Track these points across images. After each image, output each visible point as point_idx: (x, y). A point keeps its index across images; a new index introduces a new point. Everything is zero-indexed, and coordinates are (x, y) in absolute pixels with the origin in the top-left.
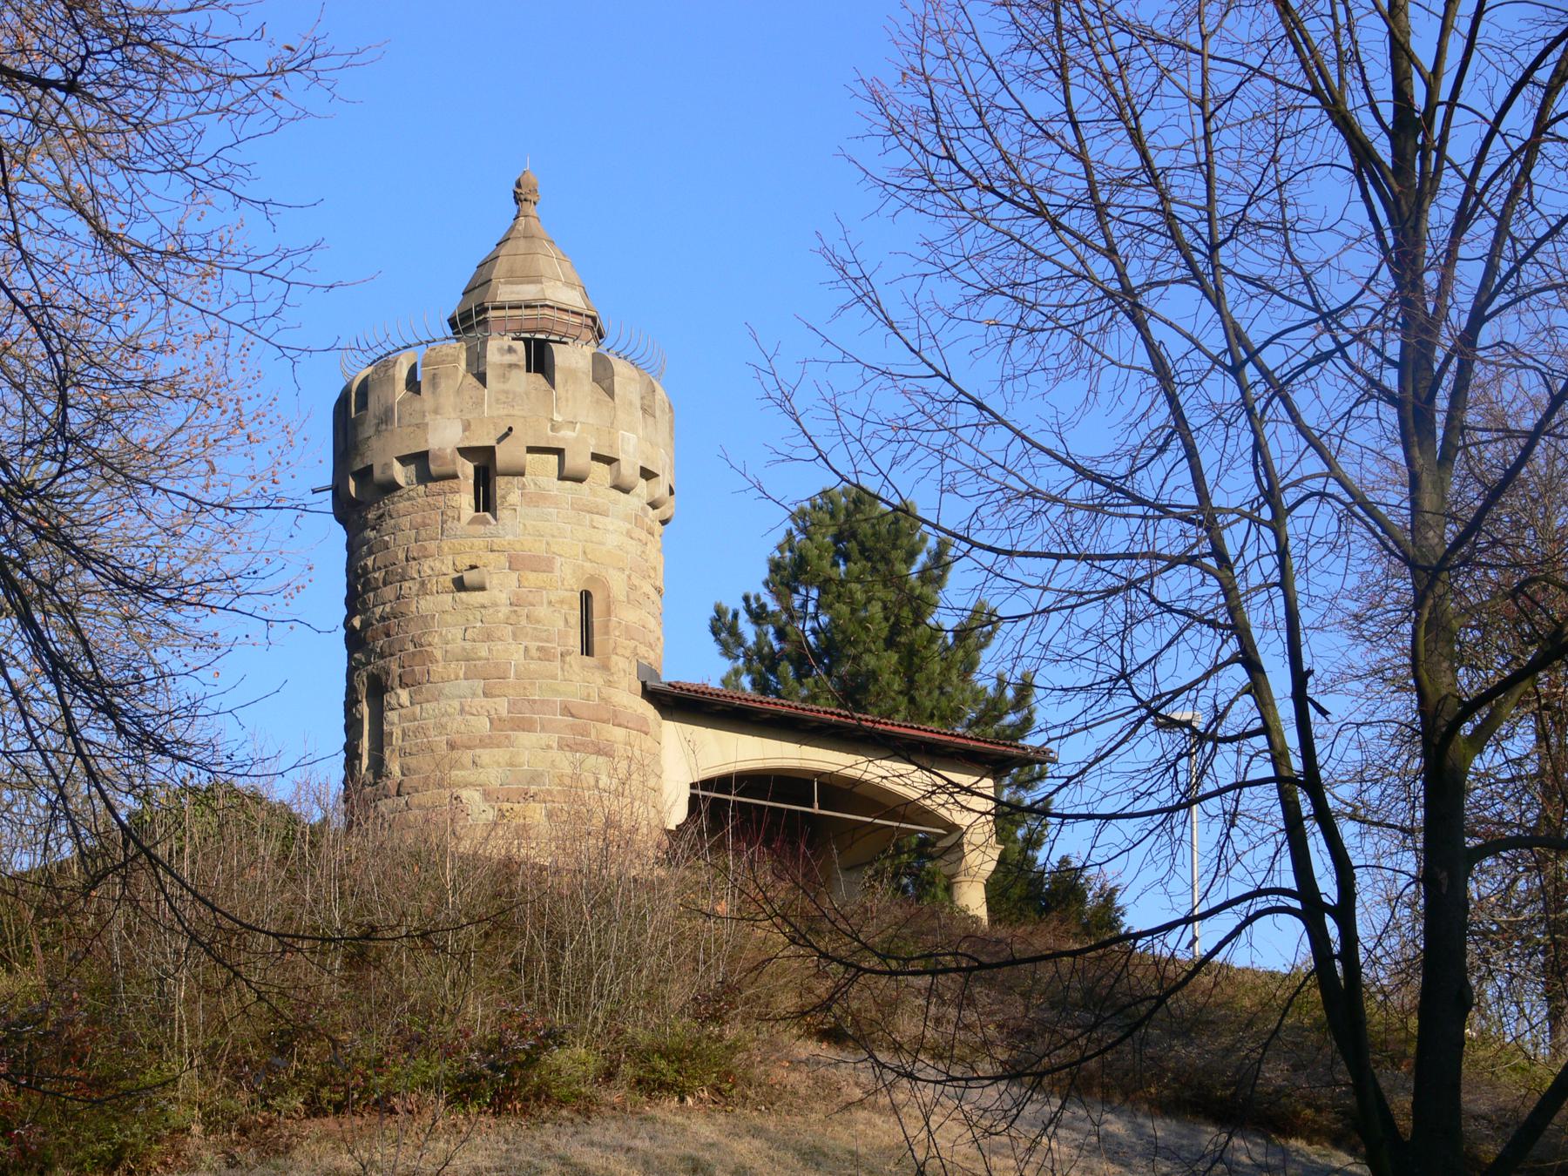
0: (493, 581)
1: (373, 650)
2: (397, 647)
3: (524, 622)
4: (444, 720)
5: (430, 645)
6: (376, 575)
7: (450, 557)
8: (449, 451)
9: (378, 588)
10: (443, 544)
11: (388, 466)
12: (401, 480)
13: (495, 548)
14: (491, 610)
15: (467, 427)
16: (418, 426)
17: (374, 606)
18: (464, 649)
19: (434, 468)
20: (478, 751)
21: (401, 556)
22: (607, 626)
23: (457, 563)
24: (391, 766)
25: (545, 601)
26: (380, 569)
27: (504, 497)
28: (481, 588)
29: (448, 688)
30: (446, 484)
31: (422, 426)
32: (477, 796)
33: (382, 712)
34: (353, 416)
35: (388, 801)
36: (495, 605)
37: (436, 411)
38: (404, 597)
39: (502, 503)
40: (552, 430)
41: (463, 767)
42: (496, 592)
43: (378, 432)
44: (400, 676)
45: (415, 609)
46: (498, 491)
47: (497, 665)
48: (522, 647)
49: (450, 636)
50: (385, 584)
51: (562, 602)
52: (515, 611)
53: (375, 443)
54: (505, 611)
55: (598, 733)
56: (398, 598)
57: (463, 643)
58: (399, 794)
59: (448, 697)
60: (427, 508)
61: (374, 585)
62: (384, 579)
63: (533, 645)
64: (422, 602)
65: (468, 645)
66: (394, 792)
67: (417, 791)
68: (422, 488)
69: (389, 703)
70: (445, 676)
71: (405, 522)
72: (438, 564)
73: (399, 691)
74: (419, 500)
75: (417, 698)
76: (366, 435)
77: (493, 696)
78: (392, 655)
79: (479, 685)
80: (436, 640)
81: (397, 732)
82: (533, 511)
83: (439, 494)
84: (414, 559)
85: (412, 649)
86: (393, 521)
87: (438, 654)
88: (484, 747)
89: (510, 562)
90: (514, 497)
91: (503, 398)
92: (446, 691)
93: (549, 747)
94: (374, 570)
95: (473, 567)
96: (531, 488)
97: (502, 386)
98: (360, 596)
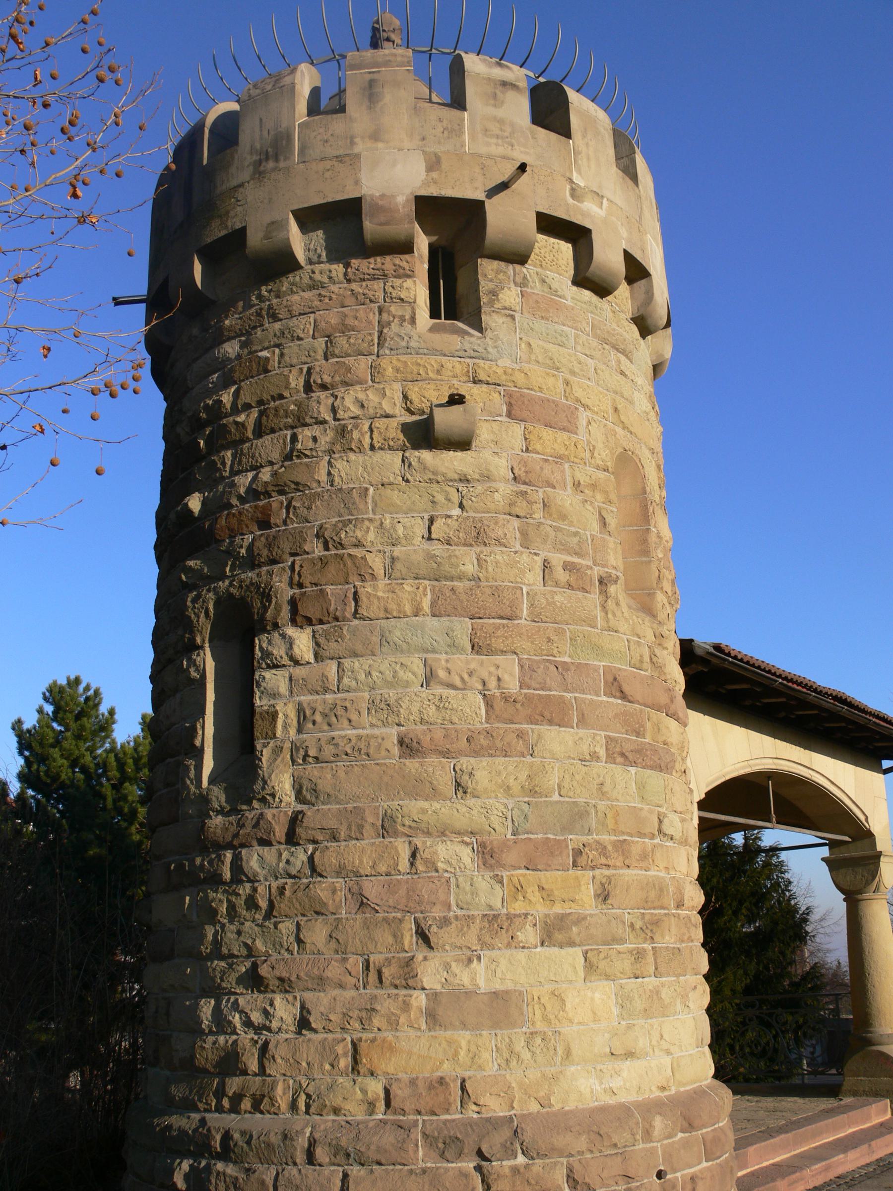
0: (484, 433)
1: (230, 553)
2: (286, 546)
3: (538, 515)
4: (391, 694)
5: (358, 544)
6: (241, 418)
7: (398, 386)
8: (401, 199)
9: (244, 440)
10: (384, 362)
11: (279, 225)
12: (300, 255)
13: (482, 376)
14: (479, 488)
15: (434, 164)
16: (339, 158)
17: (234, 473)
18: (431, 557)
19: (370, 226)
20: (465, 762)
21: (296, 381)
22: (645, 541)
23: (413, 396)
24: (274, 781)
25: (569, 480)
26: (247, 407)
27: (494, 293)
28: (463, 444)
29: (397, 630)
30: (389, 262)
31: (350, 160)
32: (466, 854)
33: (251, 672)
34: (205, 162)
35: (269, 854)
36: (487, 477)
37: (375, 136)
38: (301, 455)
39: (491, 303)
40: (573, 196)
41: (434, 794)
42: (487, 454)
43: (259, 174)
44: (293, 602)
45: (323, 477)
46: (482, 282)
47: (496, 592)
48: (539, 560)
49: (400, 530)
50: (259, 432)
51: (594, 486)
52: (524, 494)
53: (252, 194)
54: (504, 490)
55: (658, 728)
56: (288, 457)
57: (426, 545)
58: (291, 839)
59: (397, 648)
60: (350, 301)
61: (235, 435)
62: (258, 424)
63: (558, 559)
64: (340, 465)
65: (437, 549)
66: (280, 832)
67: (334, 838)
68: (338, 269)
69: (267, 654)
70: (392, 606)
71: (304, 325)
72: (373, 397)
73: (290, 631)
74: (334, 288)
75: (332, 647)
76: (234, 183)
77: (491, 651)
78: (274, 562)
79: (462, 628)
80: (371, 536)
81: (286, 712)
82: (540, 325)
83: (374, 278)
84: (324, 387)
85: (318, 551)
86: (277, 326)
87: (376, 563)
88: (476, 753)
89: (510, 405)
90: (510, 296)
91: (494, 128)
92: (396, 636)
93: (594, 756)
94: (236, 410)
95: (456, 400)
96: (536, 288)
97: (490, 111)
98: (203, 458)
